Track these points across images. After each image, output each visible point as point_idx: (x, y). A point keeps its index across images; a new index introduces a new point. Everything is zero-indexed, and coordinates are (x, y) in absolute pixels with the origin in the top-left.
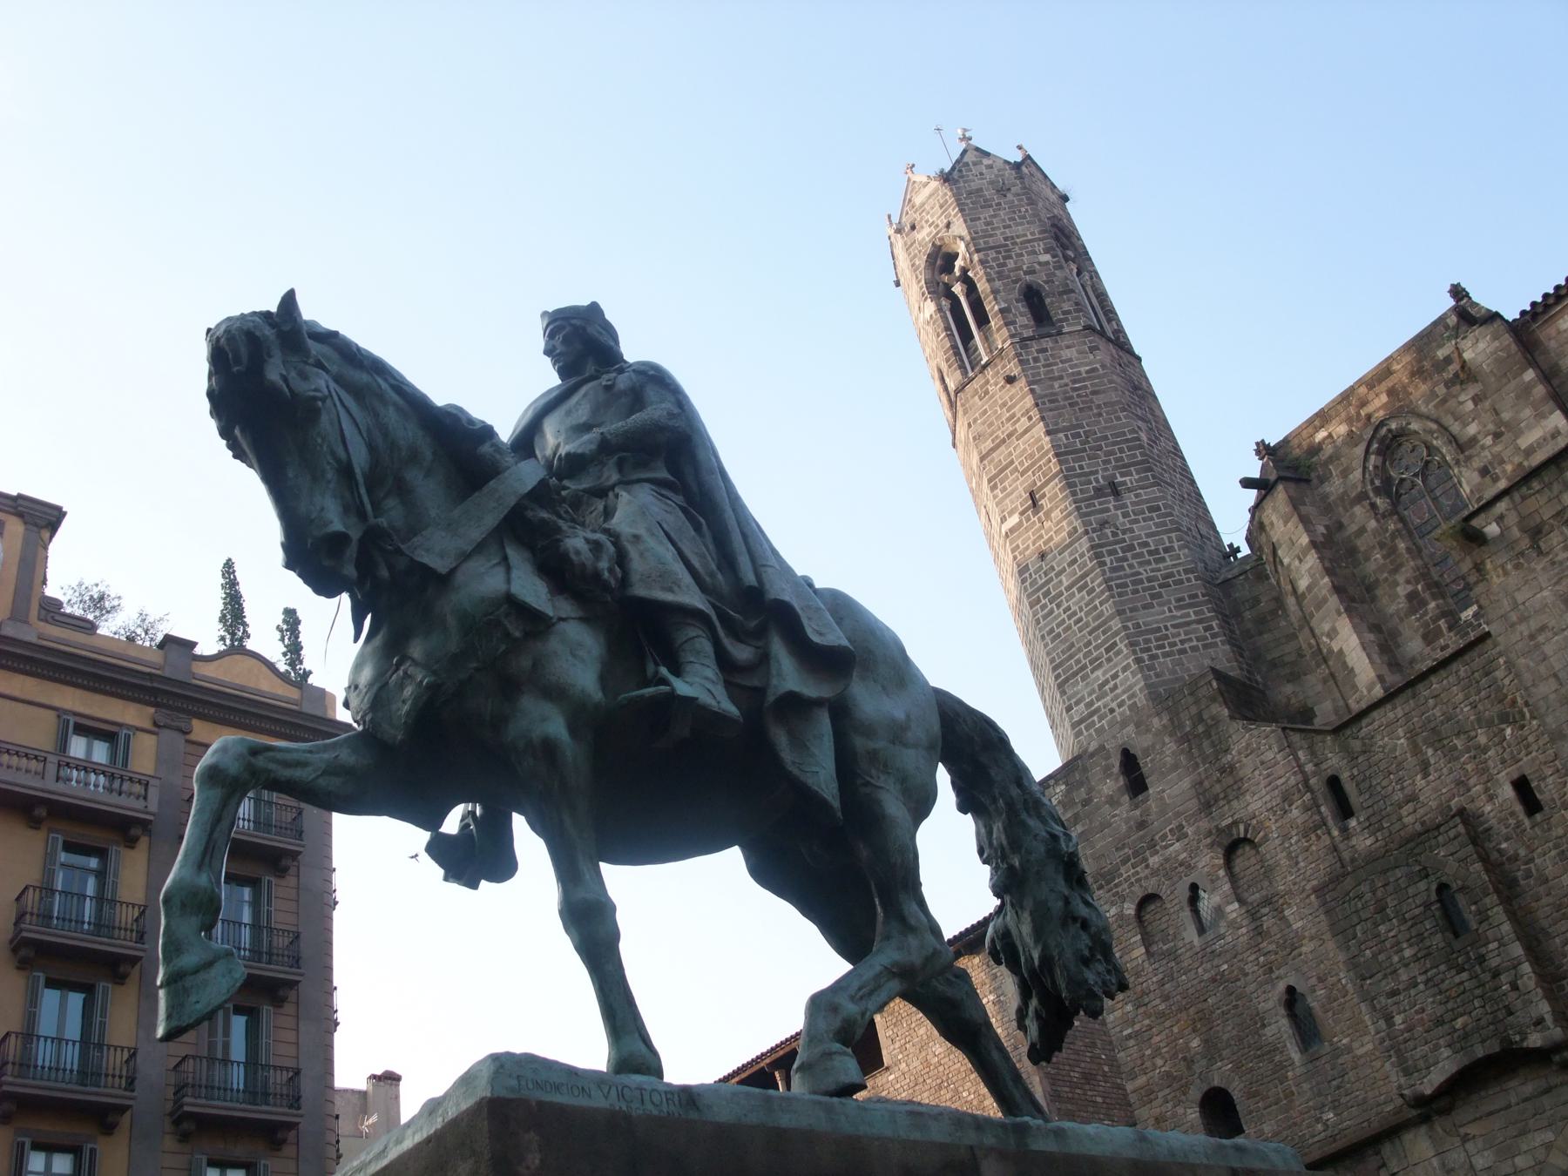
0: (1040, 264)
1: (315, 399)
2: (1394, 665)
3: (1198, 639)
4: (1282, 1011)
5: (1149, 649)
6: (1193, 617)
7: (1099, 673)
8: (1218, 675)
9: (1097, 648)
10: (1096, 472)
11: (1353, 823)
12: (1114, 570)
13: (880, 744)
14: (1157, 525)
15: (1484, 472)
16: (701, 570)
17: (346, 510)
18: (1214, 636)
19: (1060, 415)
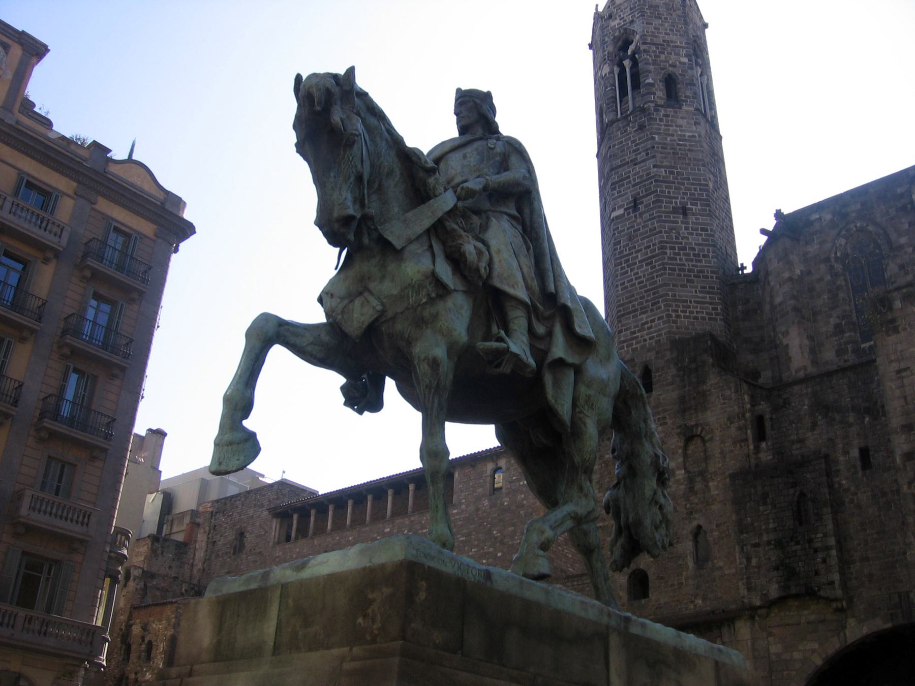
0: (680, 63)
1: (356, 135)
2: (815, 362)
3: (707, 314)
4: (691, 537)
5: (677, 311)
6: (708, 300)
7: (644, 316)
8: (713, 338)
9: (647, 301)
10: (677, 198)
11: (763, 445)
12: (670, 258)
14: (703, 240)
15: (902, 267)
16: (526, 275)
17: (355, 201)
18: (717, 314)
19: (665, 158)
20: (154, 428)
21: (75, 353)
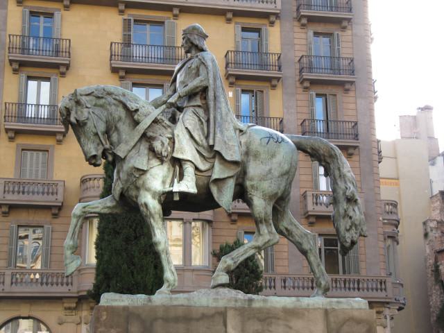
13: (254, 183)
20: (422, 106)
21: (314, 82)
